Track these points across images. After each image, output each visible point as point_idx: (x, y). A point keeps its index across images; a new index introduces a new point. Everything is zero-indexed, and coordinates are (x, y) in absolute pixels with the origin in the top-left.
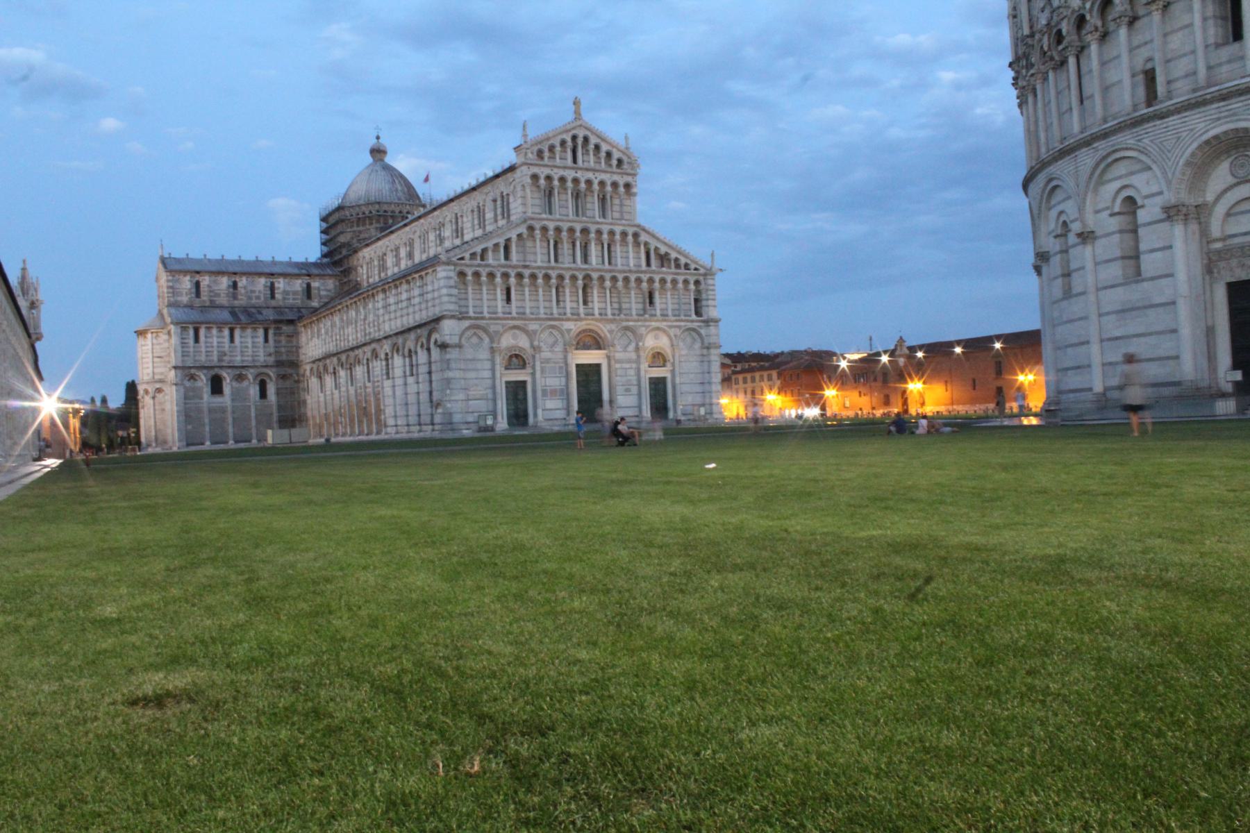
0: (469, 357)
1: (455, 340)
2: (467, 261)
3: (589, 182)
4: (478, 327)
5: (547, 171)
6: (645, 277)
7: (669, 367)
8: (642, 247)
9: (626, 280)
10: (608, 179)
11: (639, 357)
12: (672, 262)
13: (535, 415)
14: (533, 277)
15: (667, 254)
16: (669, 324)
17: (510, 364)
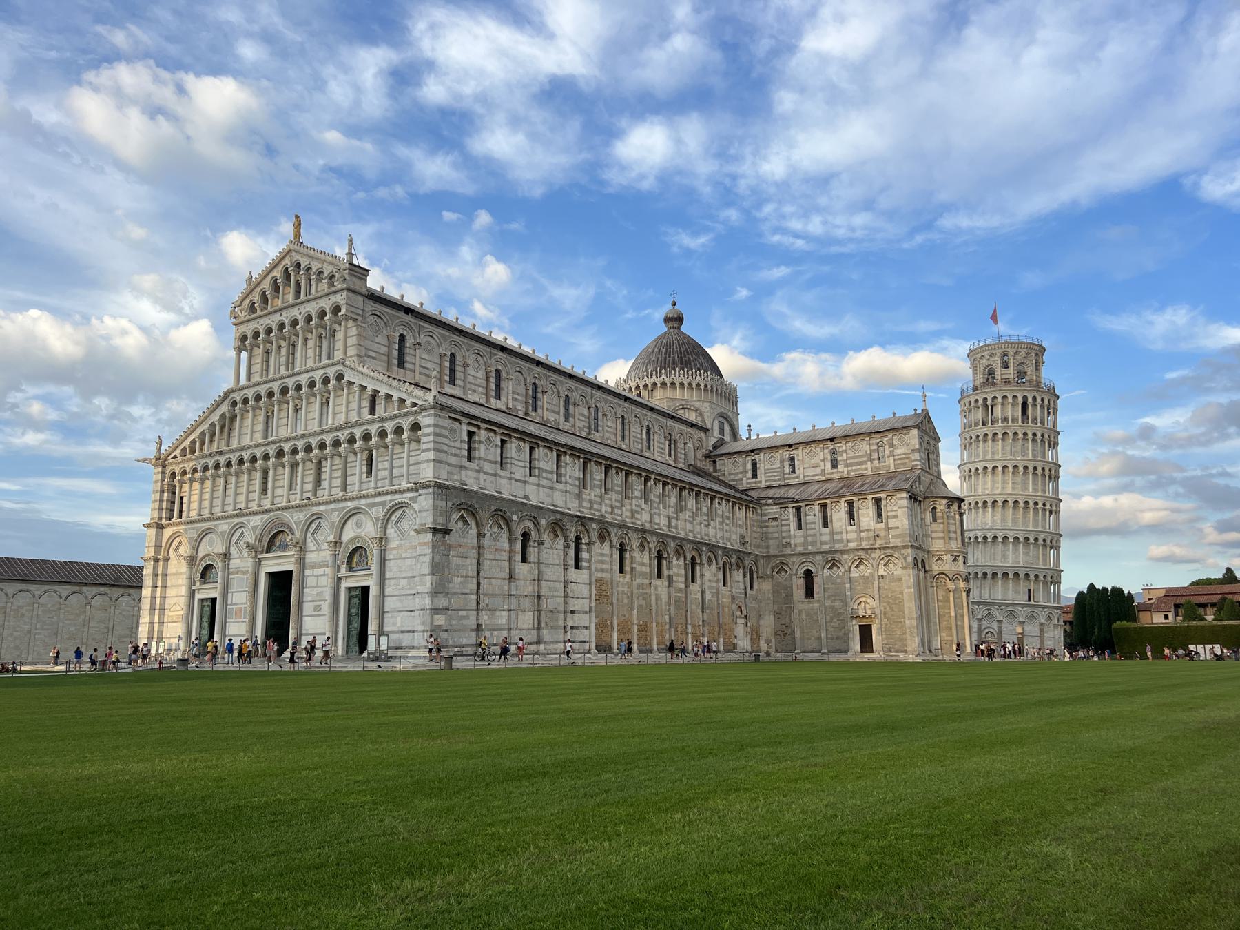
0: (174, 571)
5: (253, 326)
17: (210, 578)
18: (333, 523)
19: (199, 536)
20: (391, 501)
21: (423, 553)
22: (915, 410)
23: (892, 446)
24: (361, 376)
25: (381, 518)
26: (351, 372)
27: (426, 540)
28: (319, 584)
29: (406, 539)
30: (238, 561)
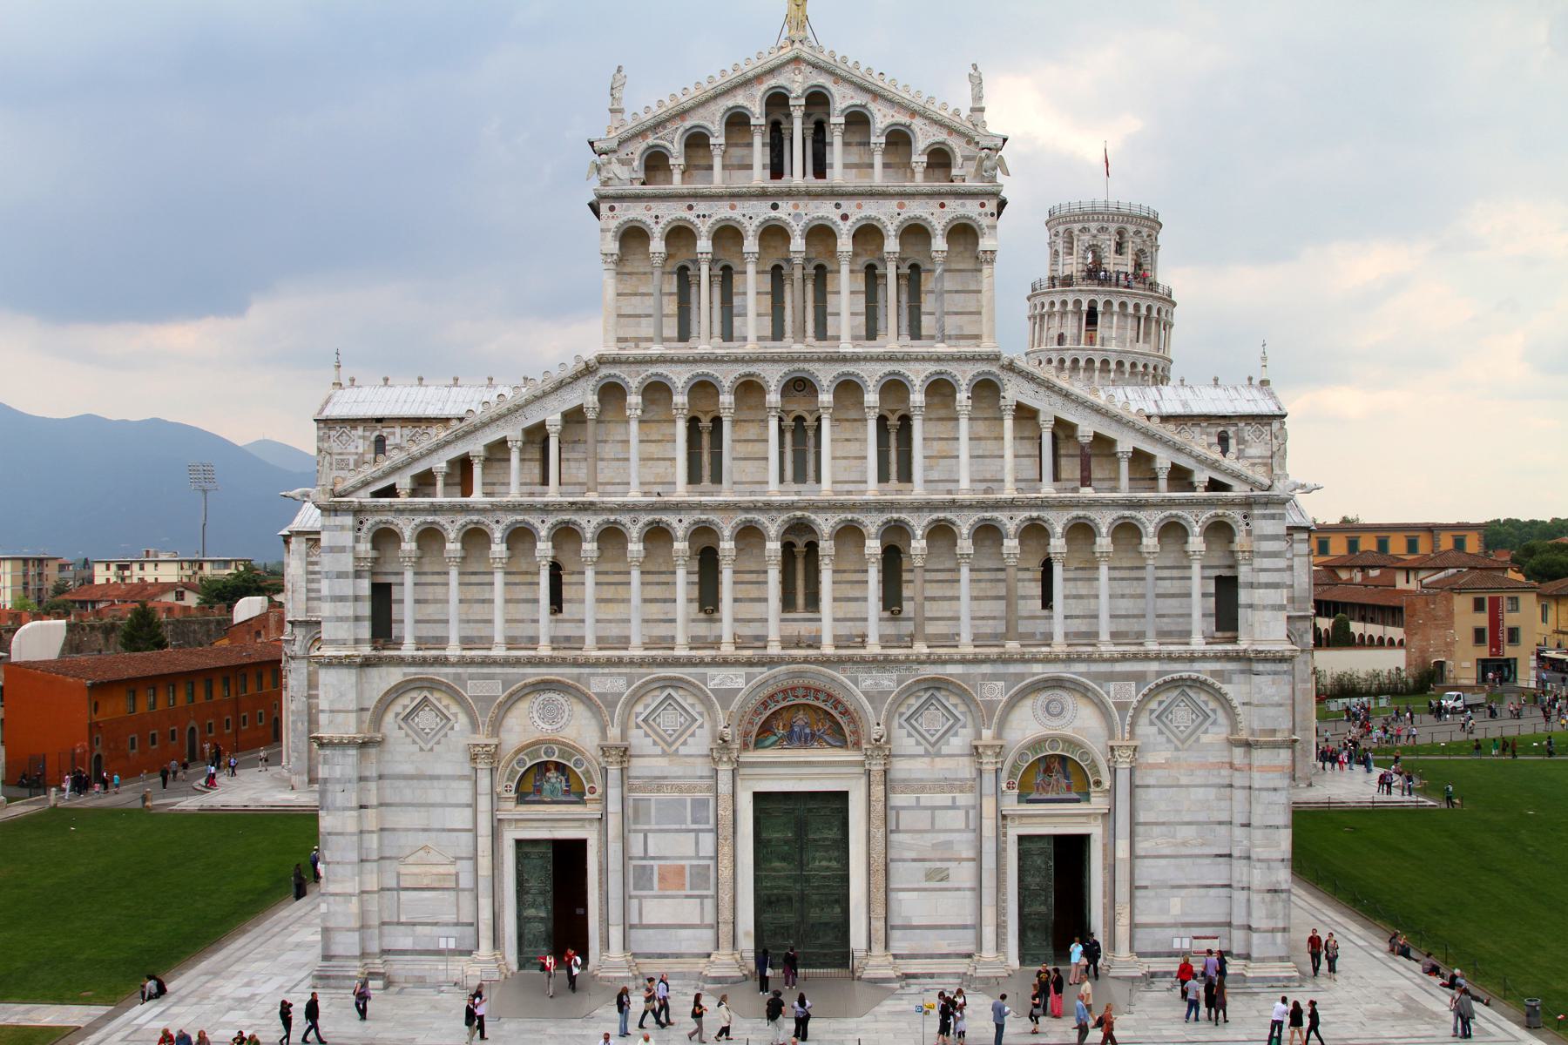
0: (408, 769)
1: (347, 727)
2: (403, 500)
3: (821, 234)
4: (432, 685)
5: (673, 212)
6: (1011, 523)
7: (1098, 803)
8: (1008, 423)
9: (941, 533)
10: (889, 215)
11: (980, 772)
12: (1124, 466)
13: (606, 944)
14: (611, 536)
15: (1103, 444)
16: (1095, 668)
17: (539, 790)
18: (990, 706)
19: (511, 695)
20: (1159, 674)
21: (1271, 785)
22: (1250, 379)
23: (1241, 441)
24: (1056, 399)
25: (1135, 704)
26: (1028, 388)
27: (1278, 762)
28: (937, 827)
29: (1186, 750)
30: (663, 762)
